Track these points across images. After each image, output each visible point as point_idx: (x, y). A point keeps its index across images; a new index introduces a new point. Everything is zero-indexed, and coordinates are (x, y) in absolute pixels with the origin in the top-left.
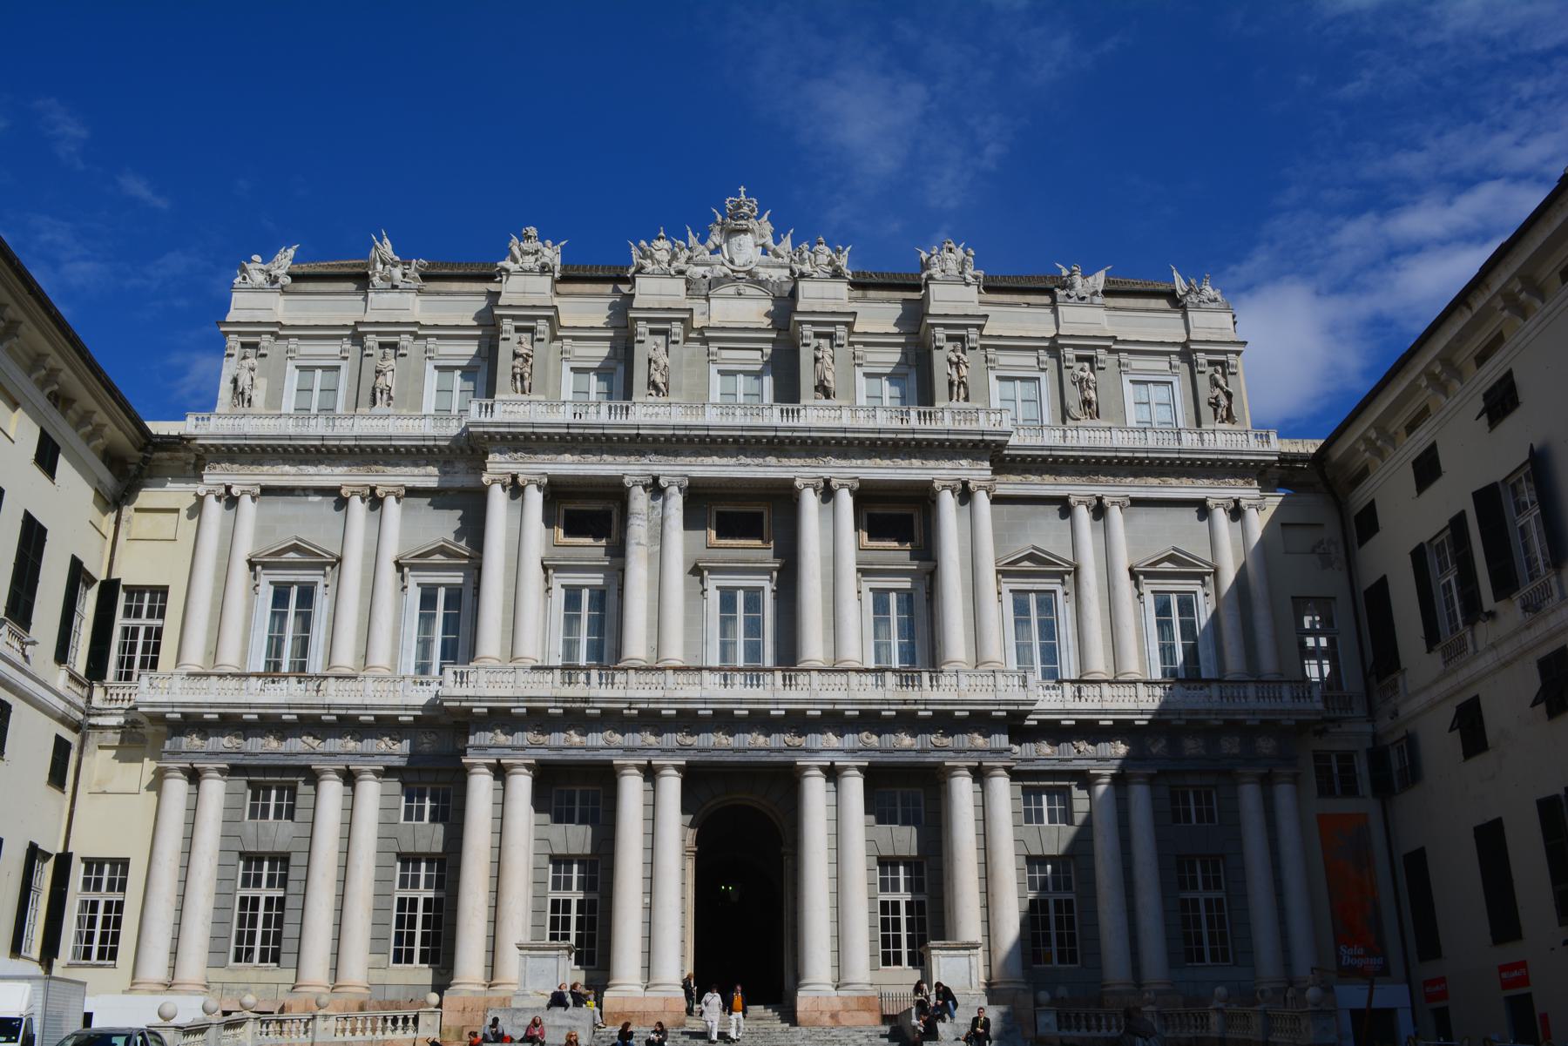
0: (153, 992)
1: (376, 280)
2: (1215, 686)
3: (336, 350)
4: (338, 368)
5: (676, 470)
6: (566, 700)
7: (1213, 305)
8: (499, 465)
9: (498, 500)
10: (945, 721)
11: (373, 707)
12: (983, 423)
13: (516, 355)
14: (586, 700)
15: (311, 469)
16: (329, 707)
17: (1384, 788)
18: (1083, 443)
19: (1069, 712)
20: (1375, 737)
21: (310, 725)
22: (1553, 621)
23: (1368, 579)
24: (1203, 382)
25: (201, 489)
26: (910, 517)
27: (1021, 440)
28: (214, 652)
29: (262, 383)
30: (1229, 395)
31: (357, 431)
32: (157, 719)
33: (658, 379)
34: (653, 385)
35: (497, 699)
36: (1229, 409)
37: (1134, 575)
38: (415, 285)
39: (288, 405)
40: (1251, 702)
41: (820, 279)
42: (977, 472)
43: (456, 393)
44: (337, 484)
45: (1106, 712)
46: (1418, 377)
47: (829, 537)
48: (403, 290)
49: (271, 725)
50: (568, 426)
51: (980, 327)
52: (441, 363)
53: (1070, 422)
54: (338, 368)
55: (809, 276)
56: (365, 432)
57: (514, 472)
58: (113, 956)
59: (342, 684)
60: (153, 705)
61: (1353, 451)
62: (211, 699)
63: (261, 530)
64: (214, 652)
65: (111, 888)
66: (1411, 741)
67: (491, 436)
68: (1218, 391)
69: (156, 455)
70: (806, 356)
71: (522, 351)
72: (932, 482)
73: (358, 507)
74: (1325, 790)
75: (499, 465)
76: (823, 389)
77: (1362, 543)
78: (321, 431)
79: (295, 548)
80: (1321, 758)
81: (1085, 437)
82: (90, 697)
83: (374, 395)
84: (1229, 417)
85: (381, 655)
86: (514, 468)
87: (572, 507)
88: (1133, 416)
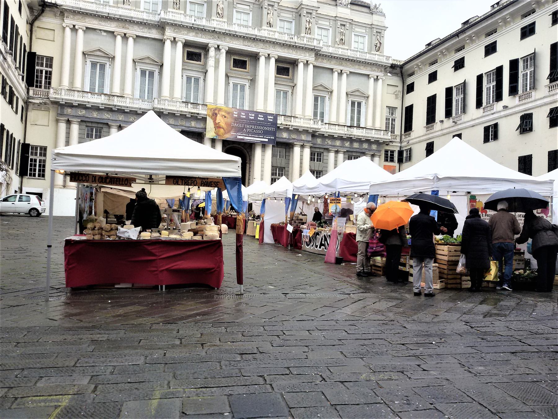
0: (60, 188)
2: (365, 129)
5: (227, 44)
6: (192, 113)
9: (168, 44)
10: (296, 131)
11: (129, 107)
12: (315, 43)
14: (198, 114)
15: (103, 23)
16: (115, 106)
17: (400, 161)
18: (340, 53)
19: (327, 132)
20: (401, 147)
21: (109, 109)
22: (460, 127)
23: (407, 104)
25: (64, 25)
26: (288, 69)
28: (72, 82)
30: (380, 43)
31: (120, 13)
32: (56, 103)
33: (220, 12)
35: (171, 110)
36: (379, 48)
37: (347, 94)
40: (373, 135)
42: (311, 58)
45: (336, 133)
46: (438, 52)
47: (266, 71)
49: (96, 108)
51: (317, 11)
53: (336, 46)
58: (43, 176)
59: (120, 99)
60: (55, 98)
61: (412, 67)
62: (76, 99)
63: (85, 43)
64: (72, 82)
65: (41, 155)
66: (410, 150)
67: (168, 23)
68: (377, 42)
69: (47, 9)
73: (119, 38)
74: (386, 160)
75: (169, 33)
76: (270, 25)
77: (407, 93)
79: (99, 50)
80: (386, 151)
81: (340, 51)
82: (28, 92)
85: (128, 91)
86: (174, 35)
87: (189, 50)
88: (354, 45)
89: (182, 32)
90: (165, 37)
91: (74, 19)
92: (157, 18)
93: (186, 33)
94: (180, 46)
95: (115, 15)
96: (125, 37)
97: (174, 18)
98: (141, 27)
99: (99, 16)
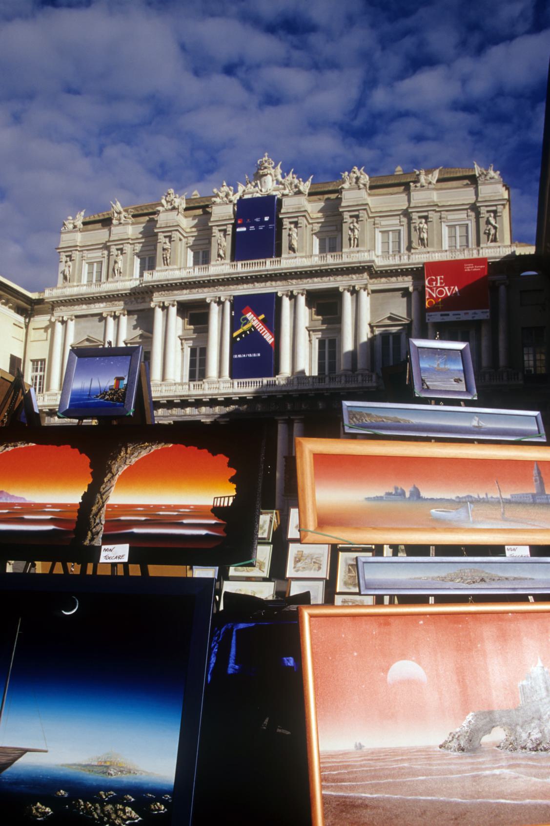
3: (100, 254)
7: (492, 181)
8: (158, 298)
9: (159, 314)
24: (482, 222)
27: (380, 262)
33: (221, 252)
34: (219, 256)
36: (495, 235)
38: (130, 221)
41: (292, 196)
55: (287, 195)
63: (77, 334)
69: (36, 307)
70: (285, 233)
72: (338, 288)
73: (111, 321)
84: (495, 240)
86: (162, 299)
90: (152, 305)
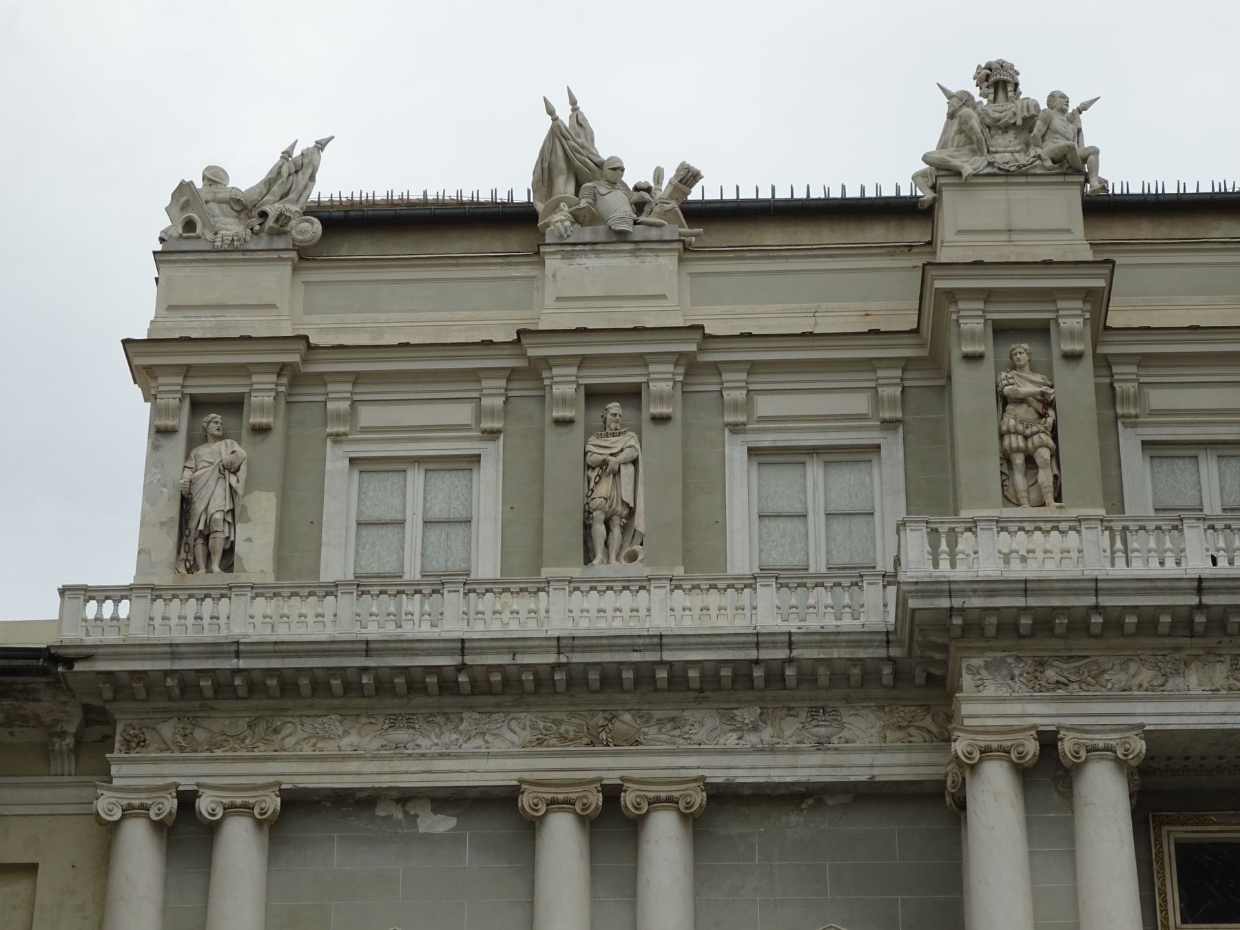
1: (558, 221)
4: (476, 459)
9: (995, 803)
13: (1004, 401)
25: (107, 805)
29: (263, 508)
31: (558, 626)
39: (336, 562)
43: (817, 521)
44: (510, 780)
48: (640, 246)
50: (1200, 586)
52: (766, 440)
54: (475, 459)
56: (584, 627)
57: (1047, 724)
71: (1027, 386)
73: (562, 840)
75: (996, 705)
78: (453, 628)
83: (587, 527)
86: (1042, 712)
89: (1117, 678)
91: (186, 746)
92: (875, 610)
93: (1146, 676)
94: (1105, 800)
95: (514, 645)
96: (613, 823)
97: (1017, 571)
98: (748, 714)
99: (384, 685)
